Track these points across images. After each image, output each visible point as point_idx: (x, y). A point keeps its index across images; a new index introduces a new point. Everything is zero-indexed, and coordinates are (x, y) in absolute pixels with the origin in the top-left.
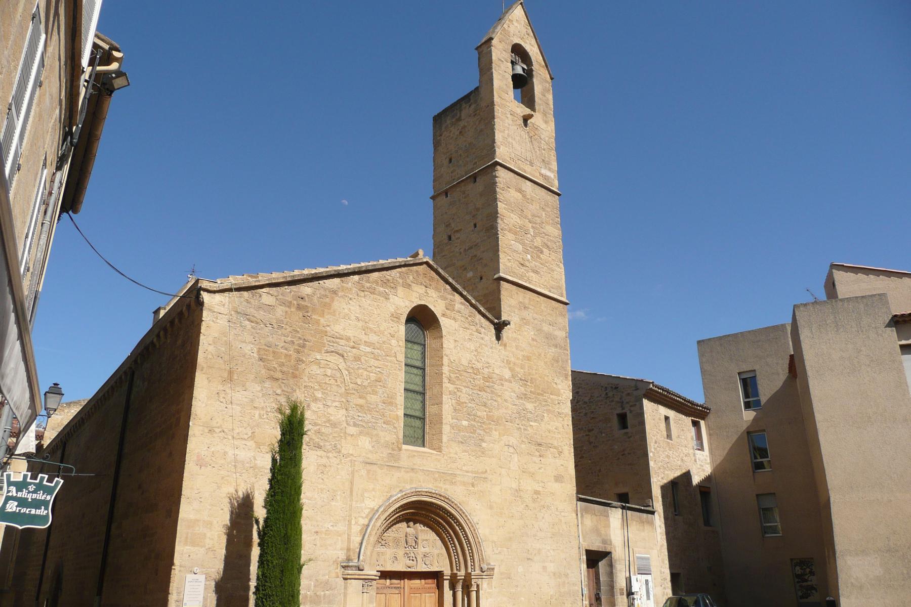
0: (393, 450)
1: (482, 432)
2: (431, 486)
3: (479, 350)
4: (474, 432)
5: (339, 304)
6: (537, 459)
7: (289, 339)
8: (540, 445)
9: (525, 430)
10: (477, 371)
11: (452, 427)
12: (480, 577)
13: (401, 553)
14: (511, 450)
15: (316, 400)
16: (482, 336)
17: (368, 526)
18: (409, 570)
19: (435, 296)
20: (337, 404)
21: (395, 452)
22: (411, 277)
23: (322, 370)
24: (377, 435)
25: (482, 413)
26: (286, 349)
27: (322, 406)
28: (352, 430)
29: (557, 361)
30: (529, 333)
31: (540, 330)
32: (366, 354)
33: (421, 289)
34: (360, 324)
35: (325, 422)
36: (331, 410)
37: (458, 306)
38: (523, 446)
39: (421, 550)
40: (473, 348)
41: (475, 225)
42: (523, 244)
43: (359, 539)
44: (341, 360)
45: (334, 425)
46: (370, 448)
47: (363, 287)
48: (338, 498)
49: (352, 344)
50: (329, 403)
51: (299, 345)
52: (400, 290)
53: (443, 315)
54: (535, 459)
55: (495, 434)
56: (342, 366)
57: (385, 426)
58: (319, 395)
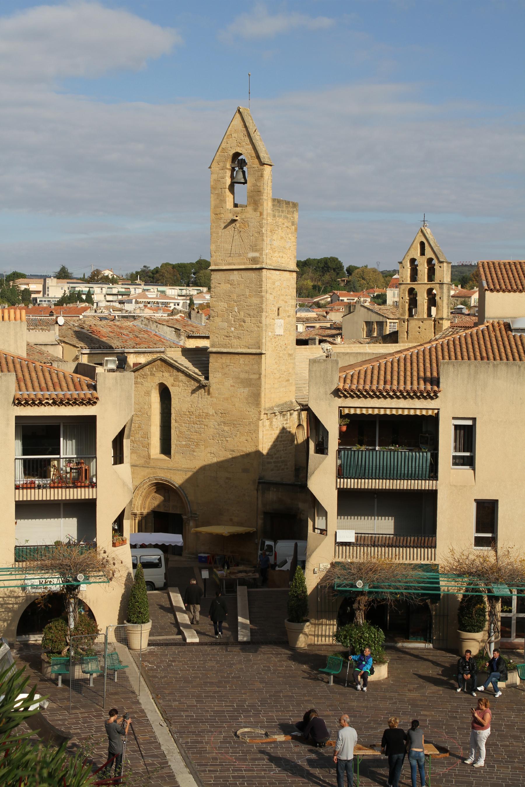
1: (194, 447)
2: (162, 475)
10: (191, 413)
11: (176, 445)
14: (213, 455)
22: (154, 369)
25: (195, 437)
30: (229, 382)
42: (228, 321)
55: (202, 447)
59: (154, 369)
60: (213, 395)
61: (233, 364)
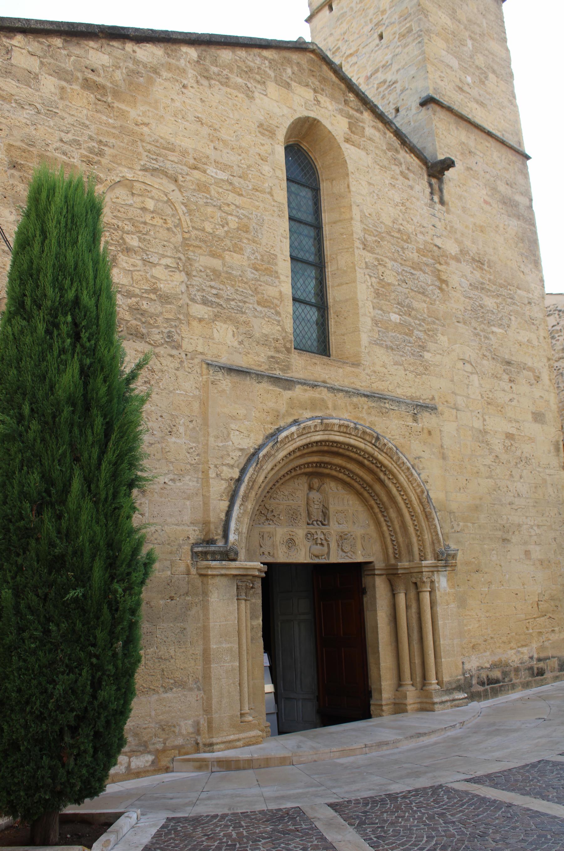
0: (277, 351)
1: (421, 335)
3: (408, 204)
4: (410, 334)
5: (163, 90)
6: (507, 387)
7: (70, 136)
8: (509, 363)
9: (486, 338)
12: (435, 569)
13: (300, 532)
14: (468, 367)
15: (128, 250)
16: (411, 183)
17: (239, 481)
18: (316, 561)
19: (330, 108)
20: (168, 261)
21: (281, 356)
22: (289, 71)
23: (138, 199)
24: (246, 323)
25: (420, 305)
26: (65, 154)
27: (140, 263)
28: (198, 310)
29: (522, 241)
31: (494, 189)
32: (218, 182)
33: (309, 94)
34: (205, 131)
35: (146, 291)
36: (158, 272)
37: (369, 131)
38: (485, 362)
39: (334, 528)
40: (397, 199)
41: (381, 37)
43: (224, 505)
44: (172, 187)
45: (165, 299)
46: (236, 344)
47: (207, 70)
48: (182, 429)
49: (192, 161)
50: (154, 259)
51: (91, 150)
52: (272, 87)
53: (347, 140)
54: (502, 384)
55: (443, 339)
56: (176, 196)
57: (259, 308)
58: (133, 241)
59: (289, 71)
60: (452, 209)
61: (481, 155)
